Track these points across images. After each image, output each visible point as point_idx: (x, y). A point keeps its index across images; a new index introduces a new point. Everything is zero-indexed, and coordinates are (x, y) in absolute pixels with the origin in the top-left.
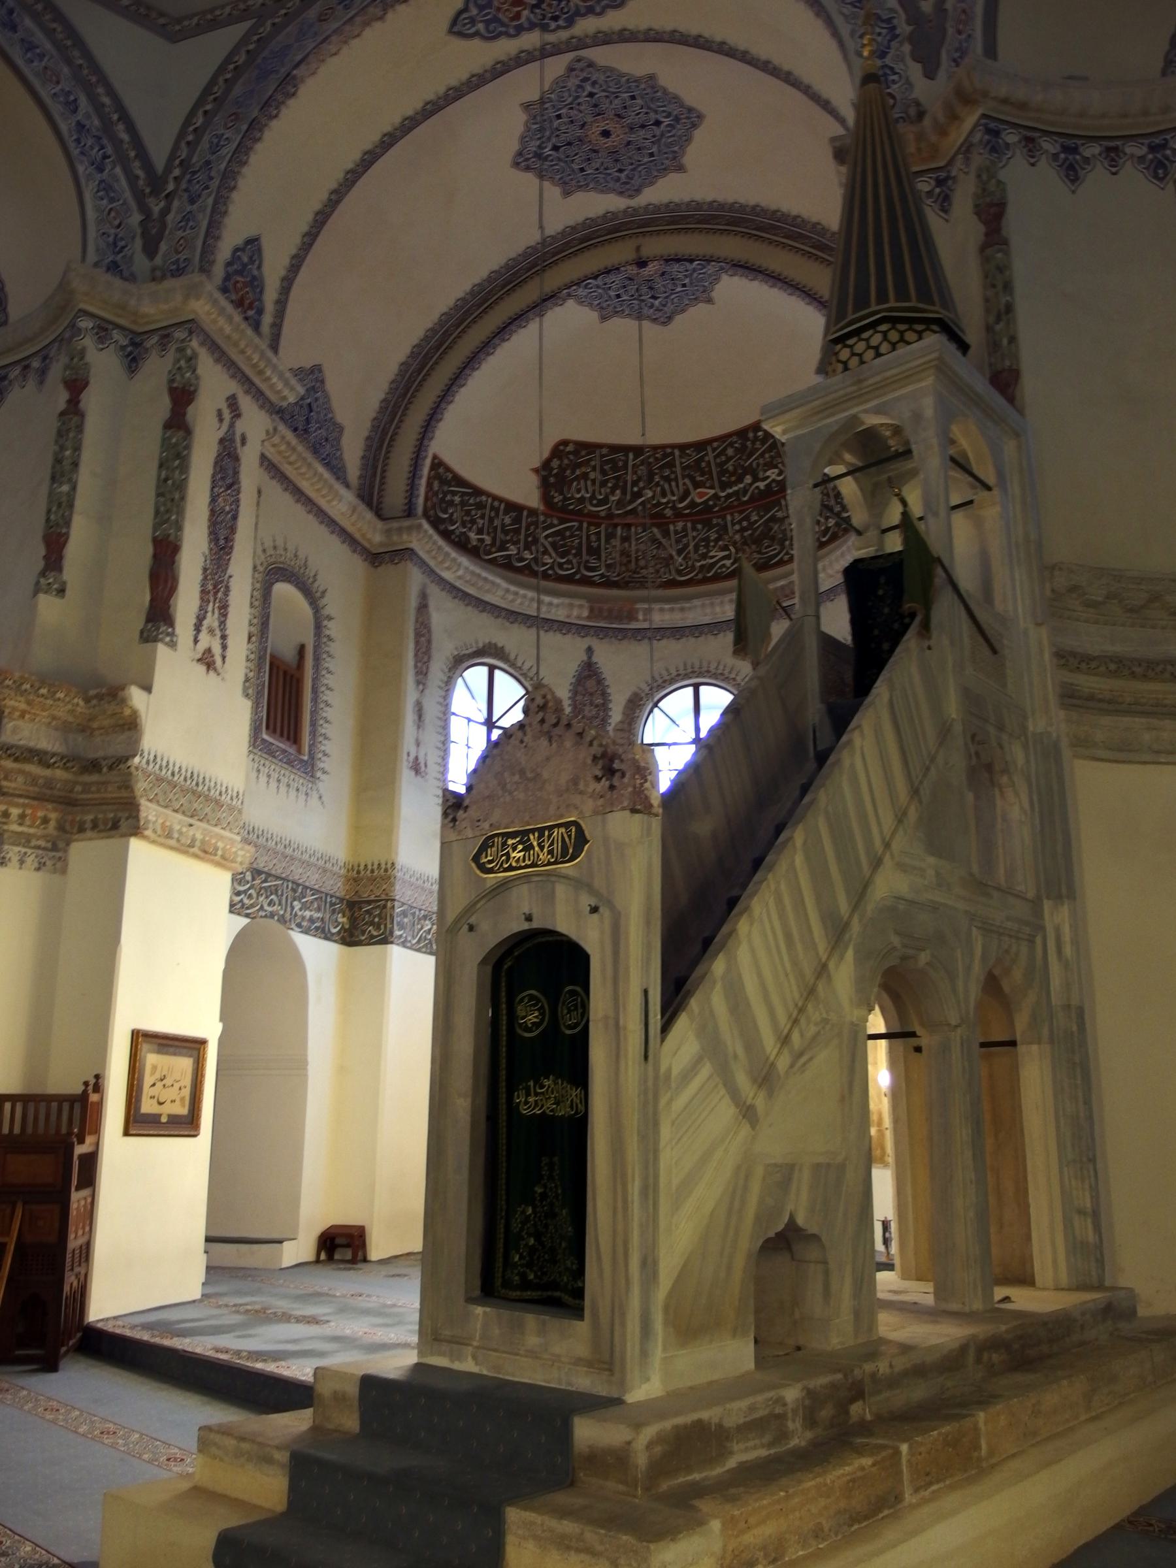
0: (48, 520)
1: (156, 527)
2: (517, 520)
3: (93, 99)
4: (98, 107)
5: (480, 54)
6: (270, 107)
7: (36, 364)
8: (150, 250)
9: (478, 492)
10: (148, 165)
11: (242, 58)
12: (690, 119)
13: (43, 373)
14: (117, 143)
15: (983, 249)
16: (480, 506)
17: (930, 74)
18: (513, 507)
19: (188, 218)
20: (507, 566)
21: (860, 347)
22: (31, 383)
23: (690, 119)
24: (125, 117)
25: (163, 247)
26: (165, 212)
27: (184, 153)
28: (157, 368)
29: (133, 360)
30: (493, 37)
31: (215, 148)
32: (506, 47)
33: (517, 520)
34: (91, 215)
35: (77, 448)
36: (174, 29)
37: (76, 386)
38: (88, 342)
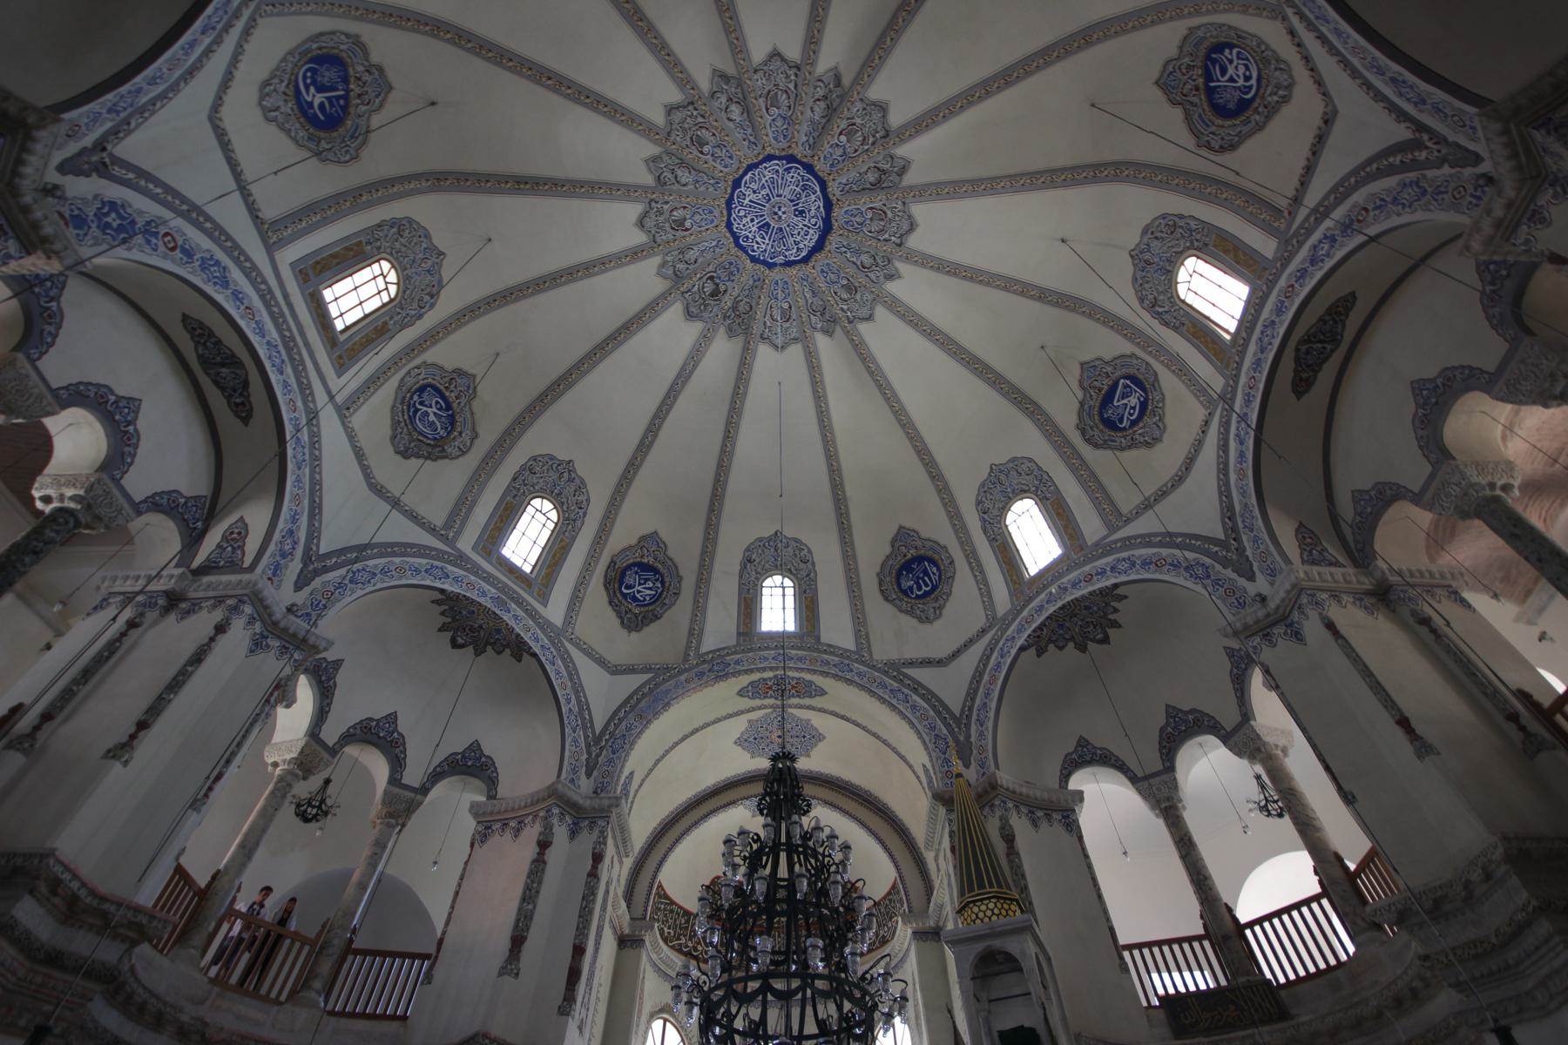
0: (516, 926)
1: (576, 937)
2: (687, 922)
3: (578, 698)
4: (579, 701)
5: (746, 703)
6: (657, 714)
7: (513, 824)
8: (589, 775)
9: (672, 902)
10: (593, 732)
11: (646, 690)
12: (821, 737)
13: (517, 832)
14: (583, 719)
15: (1008, 855)
16: (672, 911)
17: (967, 765)
18: (687, 913)
19: (610, 761)
20: (680, 951)
21: (983, 908)
22: (508, 834)
23: (821, 737)
24: (588, 709)
25: (595, 773)
26: (598, 756)
27: (612, 728)
28: (587, 839)
29: (573, 833)
30: (753, 698)
31: (629, 729)
32: (758, 702)
33: (687, 922)
34: (567, 753)
35: (540, 883)
36: (616, 670)
37: (544, 845)
38: (555, 821)
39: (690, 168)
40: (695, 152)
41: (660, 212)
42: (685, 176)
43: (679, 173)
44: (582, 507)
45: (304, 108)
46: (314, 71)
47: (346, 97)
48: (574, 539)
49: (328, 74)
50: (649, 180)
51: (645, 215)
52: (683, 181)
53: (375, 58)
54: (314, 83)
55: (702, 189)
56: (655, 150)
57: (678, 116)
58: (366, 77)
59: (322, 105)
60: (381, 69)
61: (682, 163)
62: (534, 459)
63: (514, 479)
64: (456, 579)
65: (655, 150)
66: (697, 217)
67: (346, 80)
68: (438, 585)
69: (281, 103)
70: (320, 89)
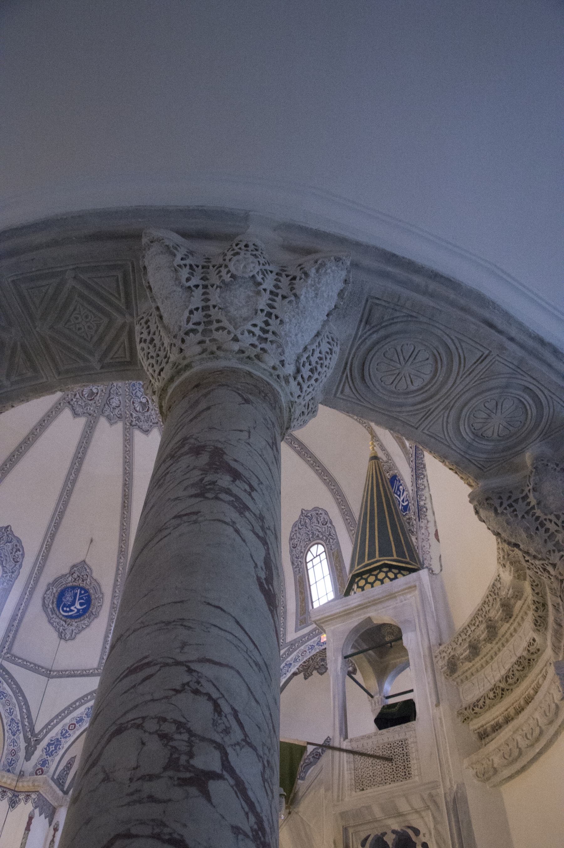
39: (109, 399)
40: (97, 398)
41: (138, 419)
42: (115, 402)
43: (114, 405)
44: (328, 522)
45: (80, 615)
46: (65, 606)
47: (82, 588)
48: (338, 543)
49: (68, 598)
50: (120, 426)
51: (140, 428)
52: (118, 402)
53: (66, 571)
54: (69, 606)
55: (120, 390)
56: (103, 421)
57: (79, 410)
58: (75, 576)
59: (81, 604)
60: (74, 566)
61: (108, 403)
62: (291, 539)
63: (293, 563)
64: (295, 660)
65: (103, 421)
66: (139, 394)
67: (73, 588)
68: (289, 675)
69: (71, 628)
70: (73, 603)
